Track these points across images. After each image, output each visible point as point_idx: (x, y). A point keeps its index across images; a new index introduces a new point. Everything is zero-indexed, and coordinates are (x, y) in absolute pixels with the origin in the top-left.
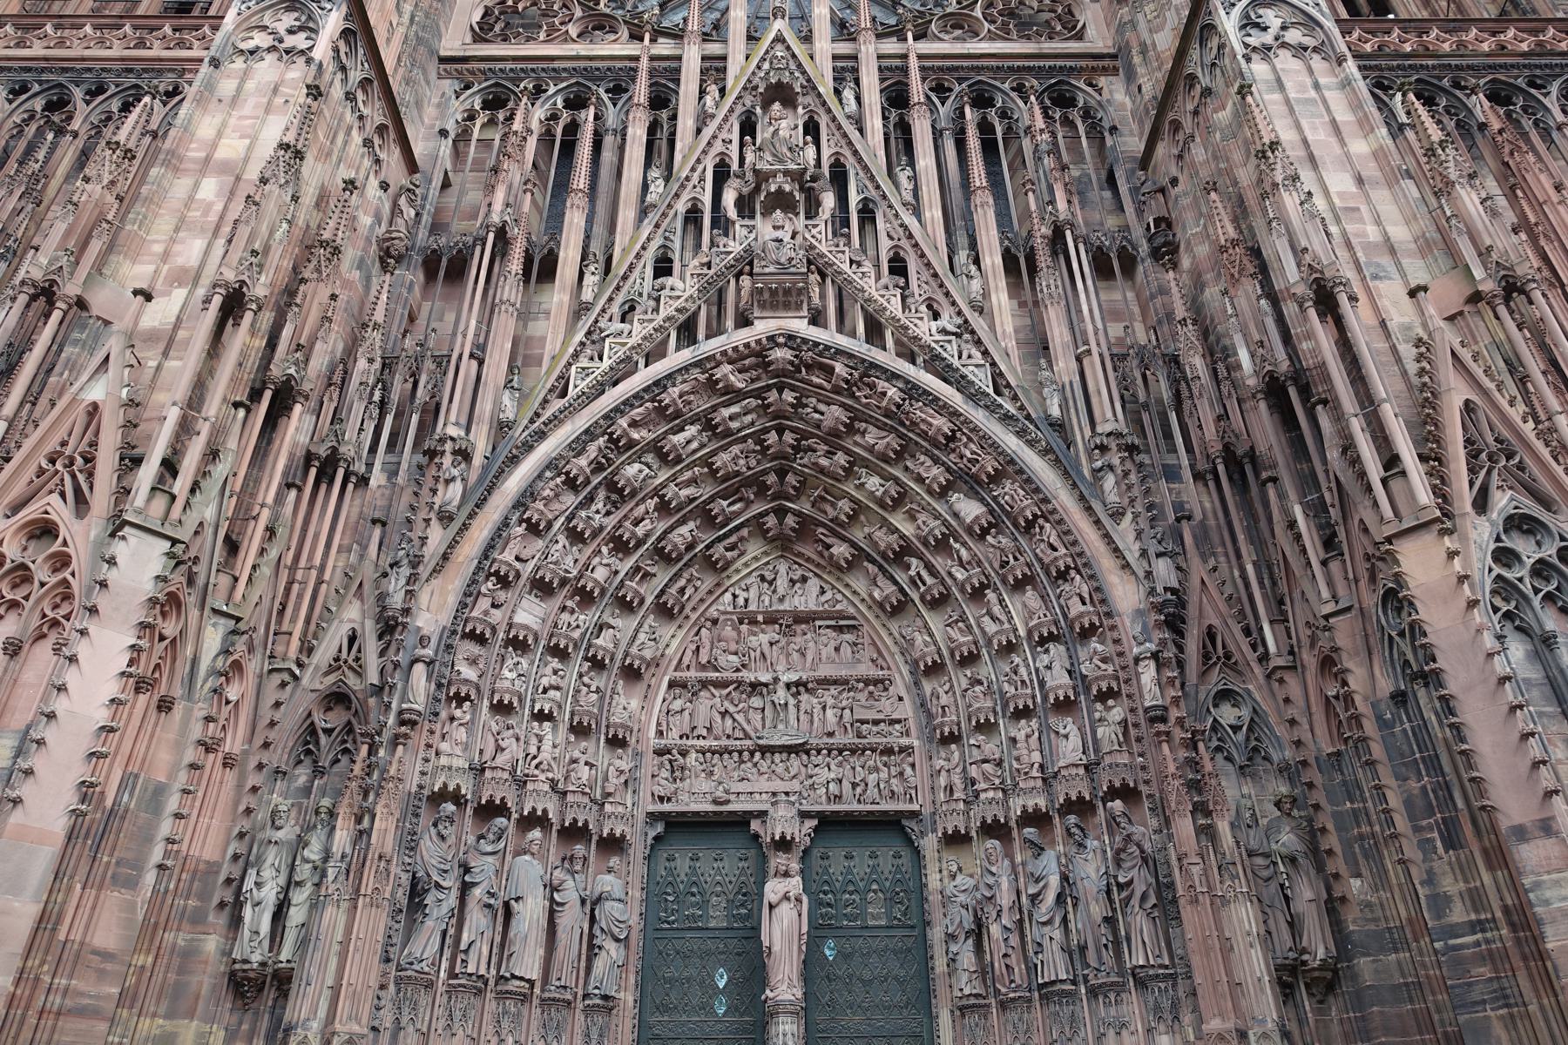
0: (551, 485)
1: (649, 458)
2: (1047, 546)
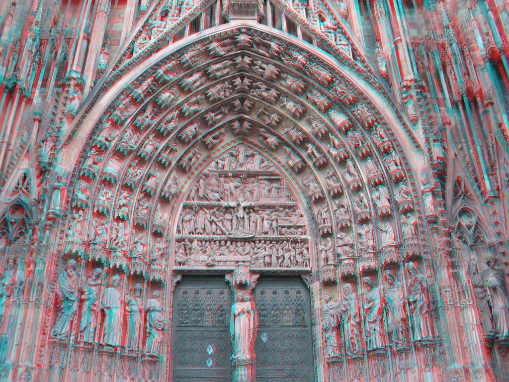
0: (124, 102)
1: (175, 90)
2: (379, 137)
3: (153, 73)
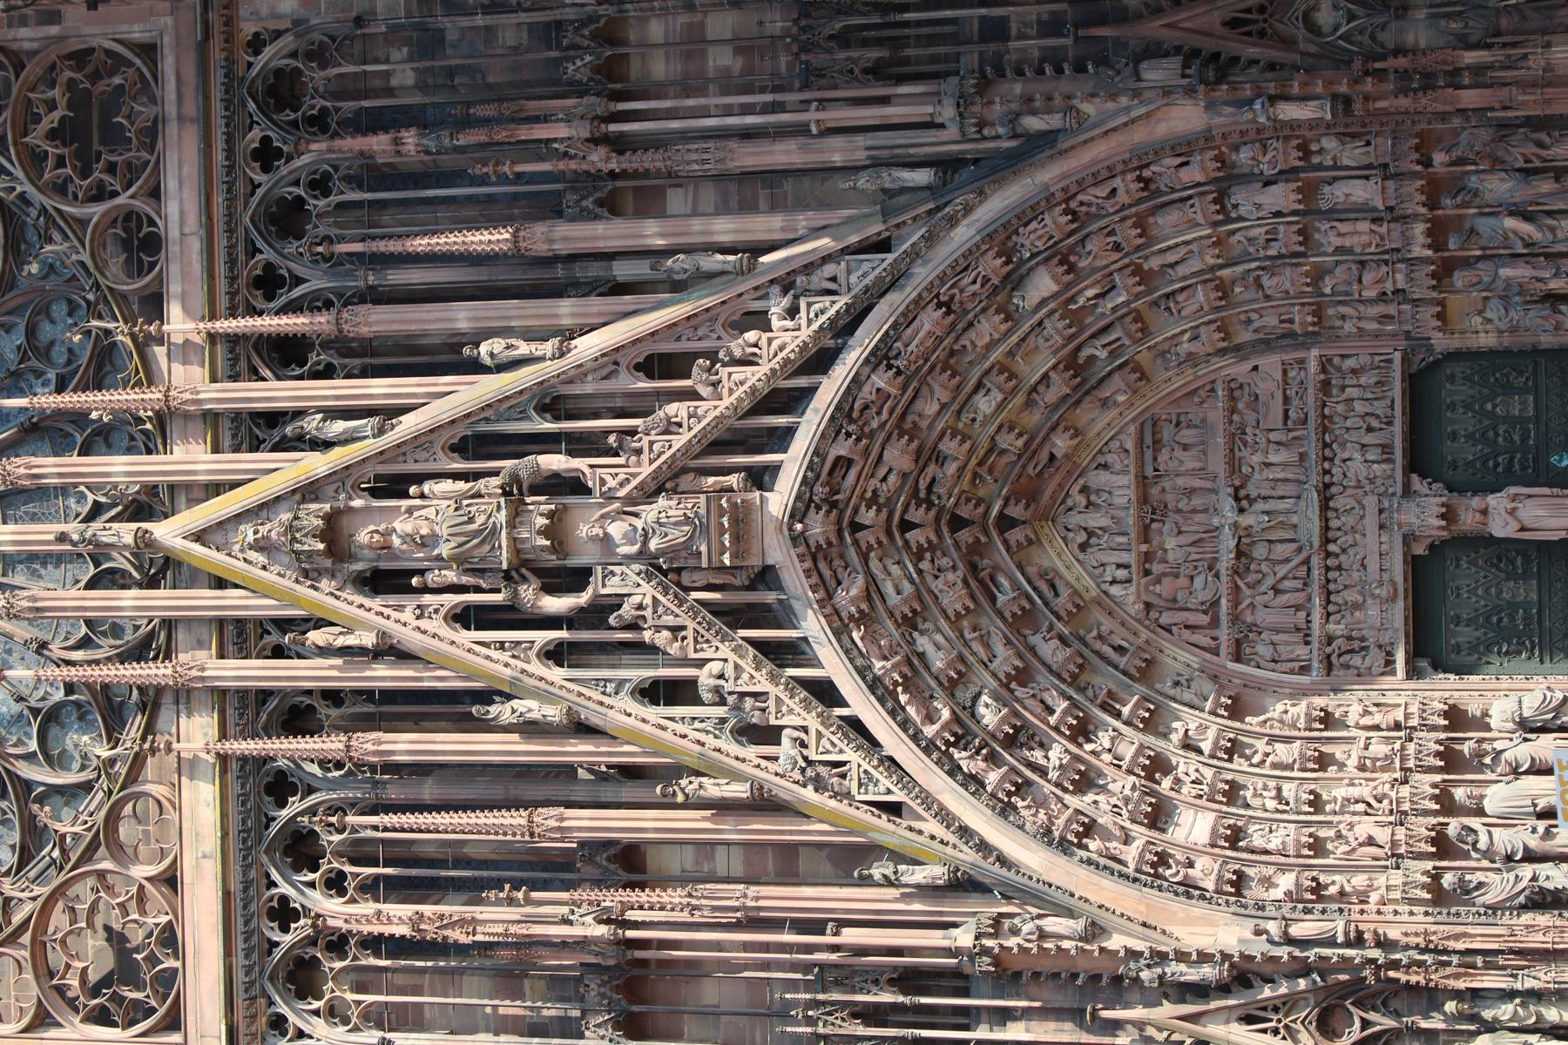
1: (964, 695)
3: (939, 749)
